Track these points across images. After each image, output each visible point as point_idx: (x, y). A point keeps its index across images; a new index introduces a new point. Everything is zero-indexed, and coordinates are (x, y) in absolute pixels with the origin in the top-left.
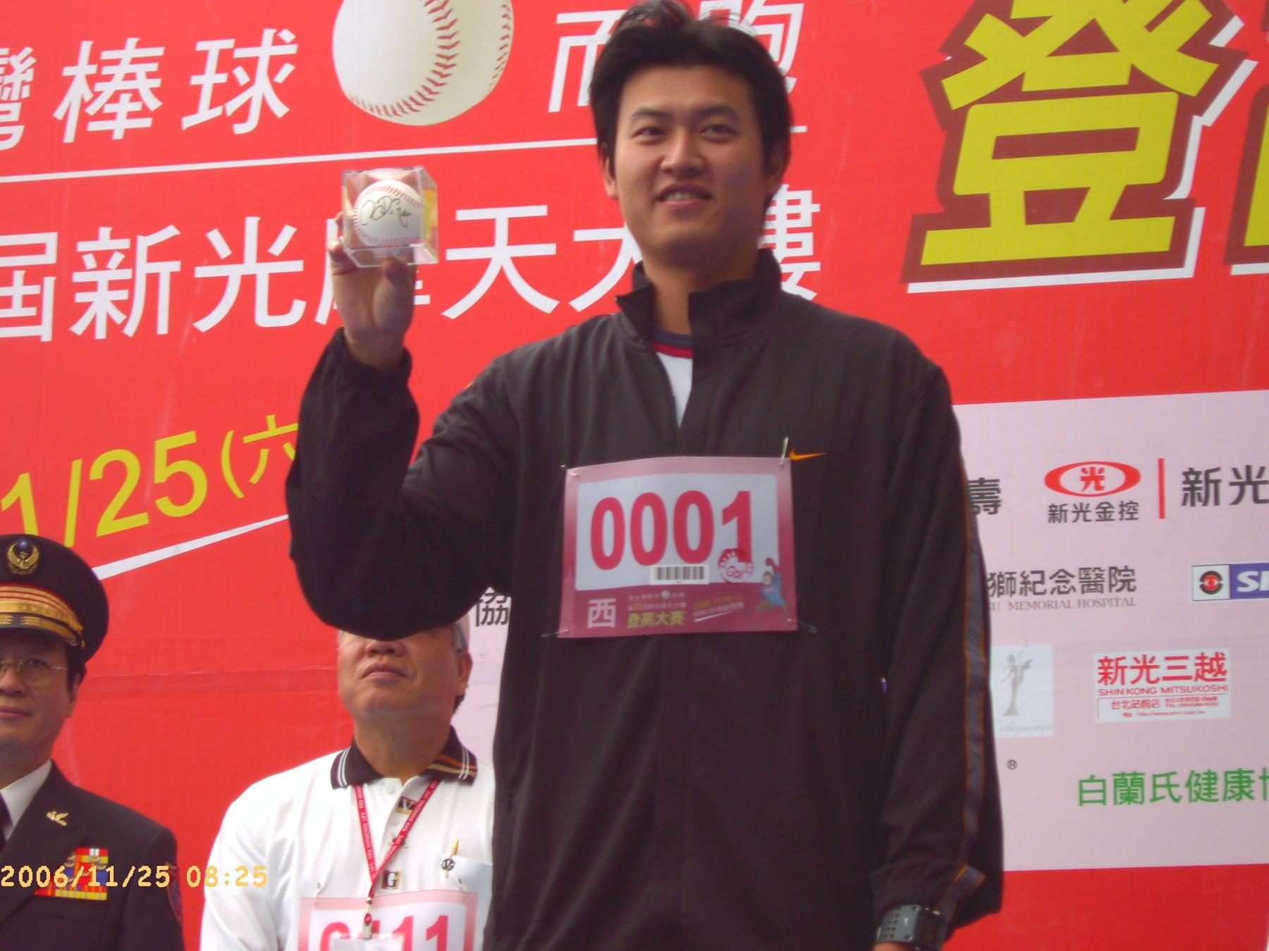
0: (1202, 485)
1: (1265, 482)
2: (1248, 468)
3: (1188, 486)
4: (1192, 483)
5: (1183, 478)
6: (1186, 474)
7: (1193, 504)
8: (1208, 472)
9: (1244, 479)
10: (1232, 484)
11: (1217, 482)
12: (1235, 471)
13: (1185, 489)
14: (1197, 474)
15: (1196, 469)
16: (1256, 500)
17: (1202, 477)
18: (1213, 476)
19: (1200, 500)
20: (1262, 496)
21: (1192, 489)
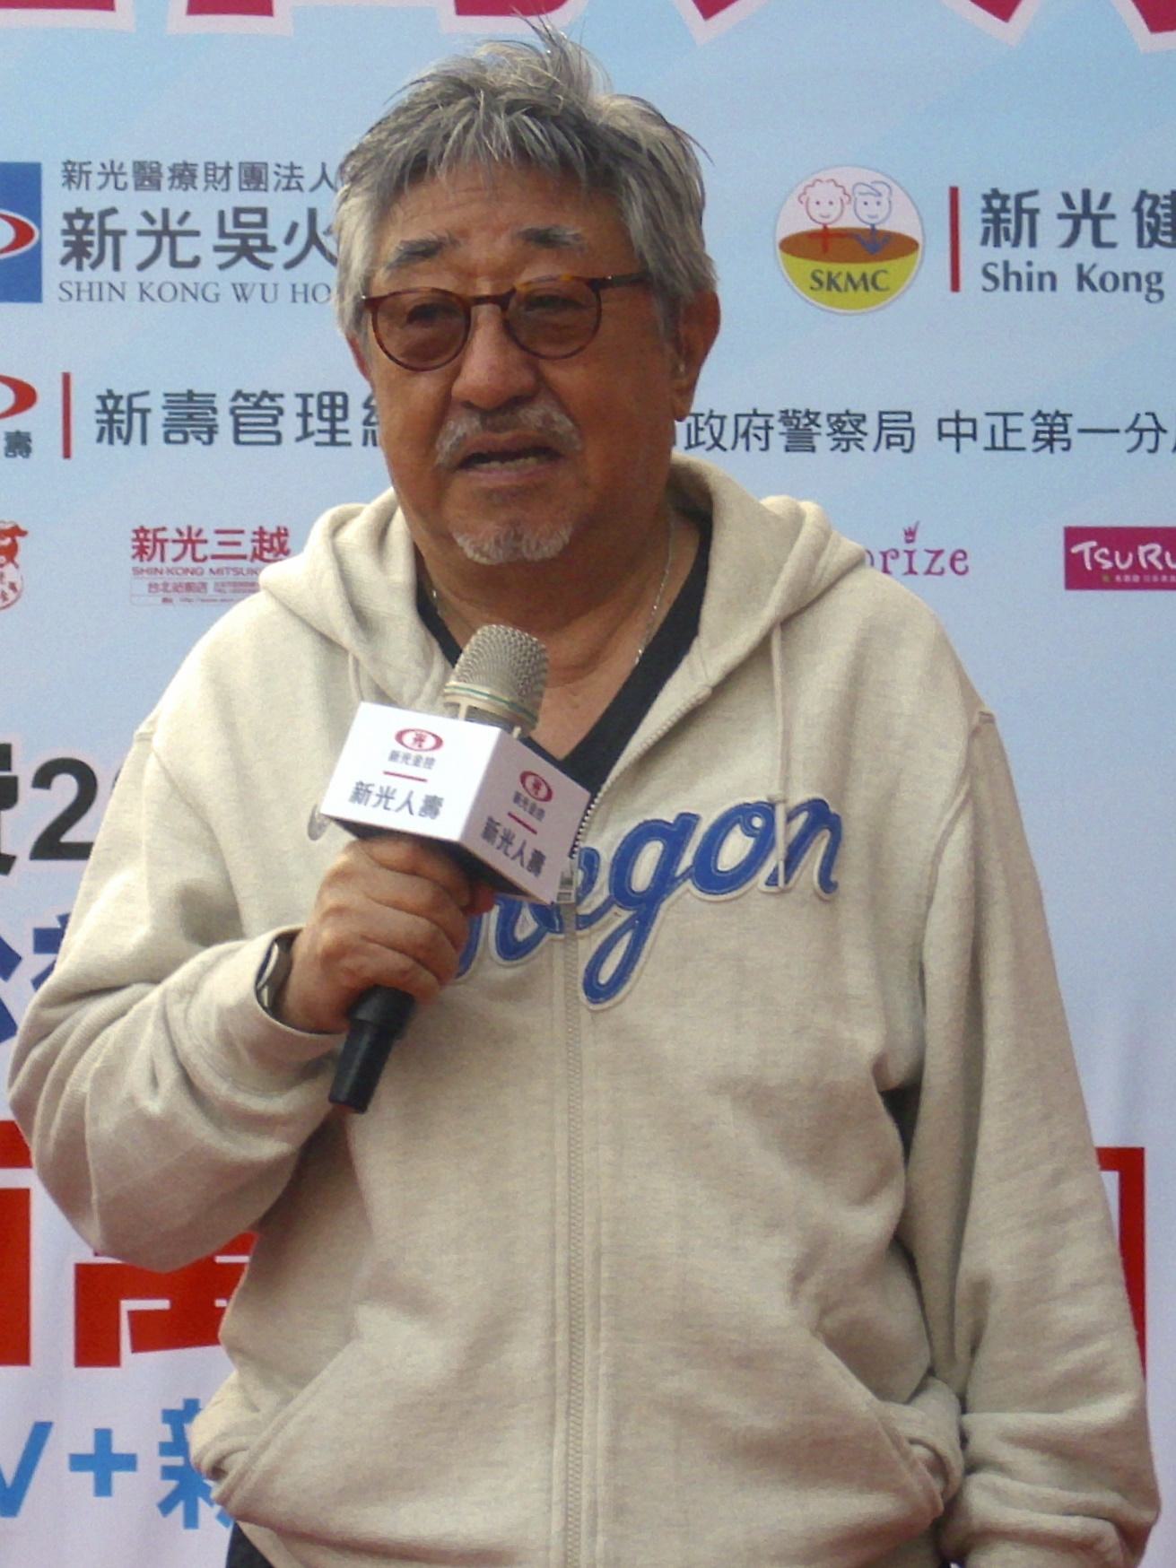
0: (1012, 216)
1: (1112, 217)
2: (1086, 195)
3: (990, 216)
4: (996, 212)
5: (983, 204)
6: (987, 198)
7: (997, 244)
8: (1019, 197)
9: (1079, 210)
10: (1061, 216)
11: (1033, 213)
12: (1067, 199)
13: (985, 221)
14: (1005, 198)
15: (1002, 191)
16: (1097, 242)
17: (1011, 204)
18: (1027, 203)
19: (1007, 238)
20: (1104, 238)
21: (997, 221)
